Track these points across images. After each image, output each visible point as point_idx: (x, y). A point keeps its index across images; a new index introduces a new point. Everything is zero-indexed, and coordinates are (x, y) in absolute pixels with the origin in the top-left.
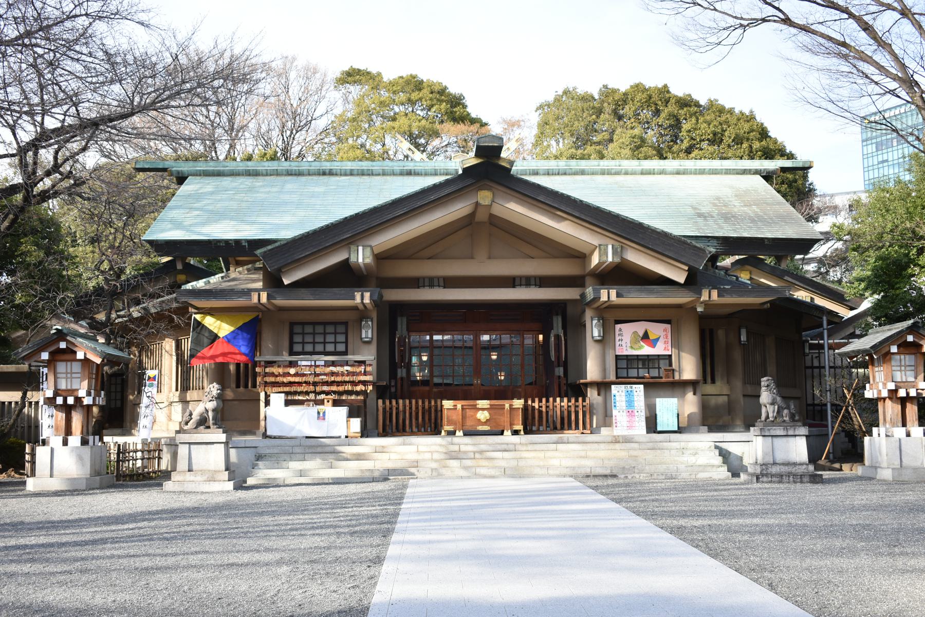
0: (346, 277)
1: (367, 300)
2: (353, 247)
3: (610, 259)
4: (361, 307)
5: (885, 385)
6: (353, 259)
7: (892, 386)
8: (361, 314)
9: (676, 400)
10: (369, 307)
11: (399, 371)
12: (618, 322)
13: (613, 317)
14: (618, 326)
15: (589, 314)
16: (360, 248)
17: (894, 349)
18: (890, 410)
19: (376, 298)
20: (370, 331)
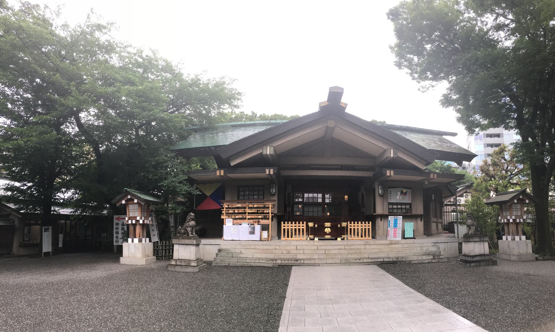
0: (261, 162)
1: (272, 173)
2: (265, 147)
3: (392, 156)
4: (270, 178)
5: (511, 218)
6: (264, 153)
7: (514, 217)
8: (269, 181)
9: (412, 224)
10: (273, 177)
11: (288, 208)
12: (390, 188)
13: (389, 186)
14: (389, 190)
15: (376, 184)
16: (268, 147)
17: (516, 201)
18: (512, 228)
19: (276, 172)
20: (274, 190)
